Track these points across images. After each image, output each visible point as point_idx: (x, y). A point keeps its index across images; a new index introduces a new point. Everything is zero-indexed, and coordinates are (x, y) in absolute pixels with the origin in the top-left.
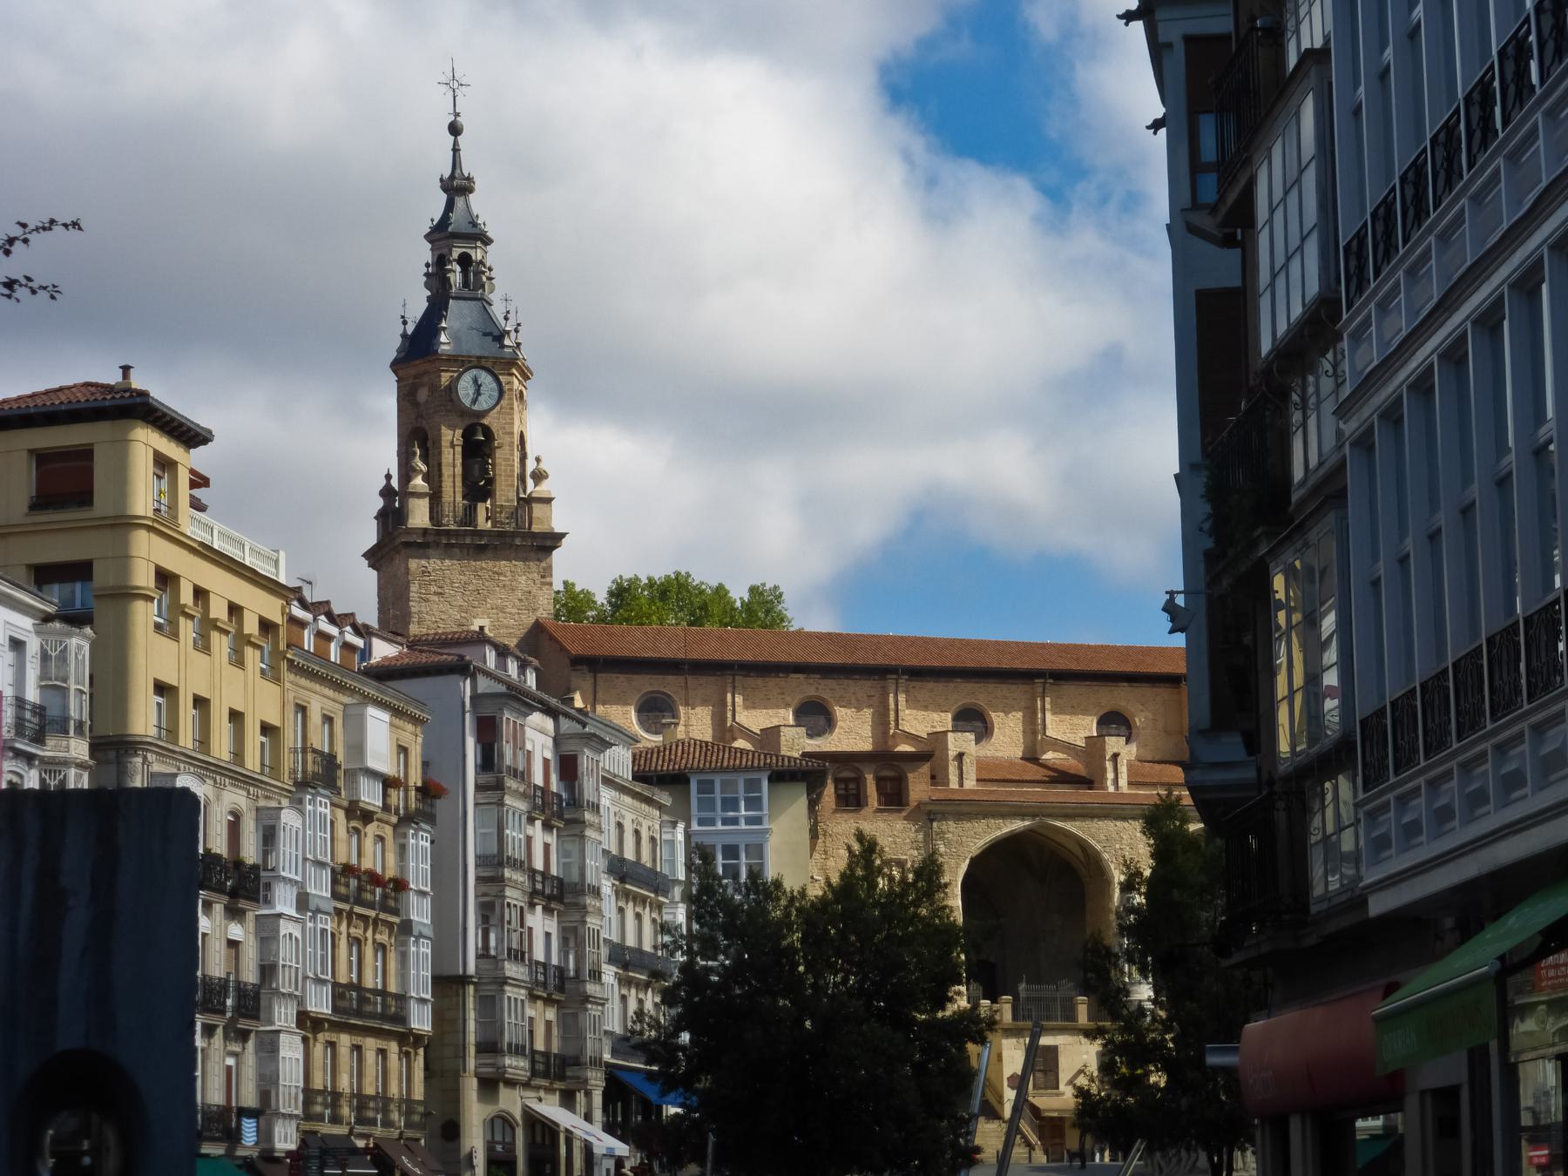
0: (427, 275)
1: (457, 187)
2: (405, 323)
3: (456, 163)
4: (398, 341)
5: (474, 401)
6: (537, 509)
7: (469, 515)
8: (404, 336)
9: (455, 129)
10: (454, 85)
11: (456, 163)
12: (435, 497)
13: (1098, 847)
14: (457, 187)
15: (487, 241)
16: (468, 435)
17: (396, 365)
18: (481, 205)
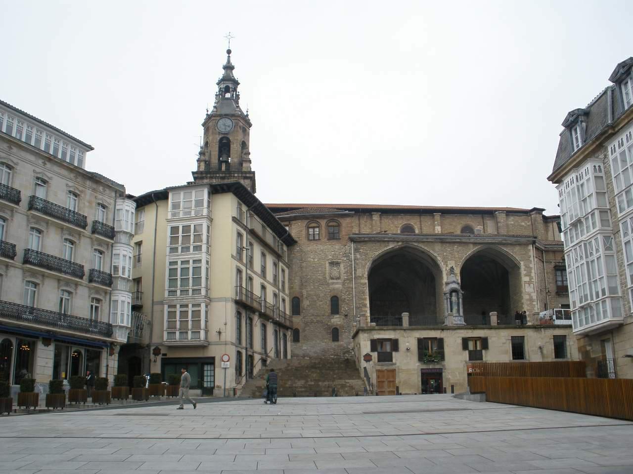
0: (216, 95)
1: (229, 67)
2: (208, 111)
3: (229, 61)
4: (205, 117)
5: (225, 129)
6: (244, 165)
7: (220, 168)
8: (207, 115)
9: (229, 52)
10: (229, 37)
11: (229, 61)
12: (208, 163)
13: (435, 254)
14: (229, 67)
15: (238, 84)
16: (221, 140)
17: (204, 125)
18: (236, 74)
